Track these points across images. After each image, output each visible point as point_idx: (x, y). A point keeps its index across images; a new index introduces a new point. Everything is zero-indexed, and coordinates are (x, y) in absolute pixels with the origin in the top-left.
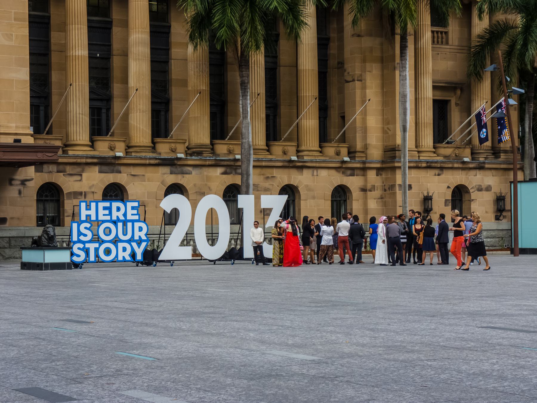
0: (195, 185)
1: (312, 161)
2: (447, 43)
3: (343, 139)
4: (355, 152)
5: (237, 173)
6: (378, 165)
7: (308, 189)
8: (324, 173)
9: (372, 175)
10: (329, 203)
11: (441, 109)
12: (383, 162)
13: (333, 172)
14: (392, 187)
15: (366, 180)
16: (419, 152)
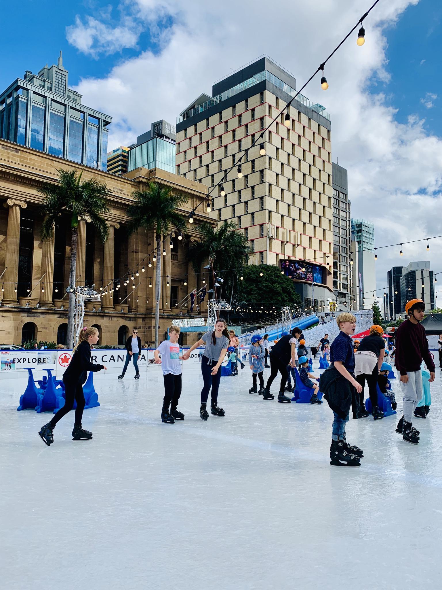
0: (42, 323)
1: (109, 313)
2: (177, 260)
3: (126, 302)
4: (132, 309)
5: (66, 318)
6: (143, 316)
7: (107, 327)
8: (115, 319)
9: (140, 321)
10: (117, 334)
11: (174, 290)
12: (145, 315)
13: (121, 319)
14: (150, 327)
15: (137, 323)
16: (164, 310)
